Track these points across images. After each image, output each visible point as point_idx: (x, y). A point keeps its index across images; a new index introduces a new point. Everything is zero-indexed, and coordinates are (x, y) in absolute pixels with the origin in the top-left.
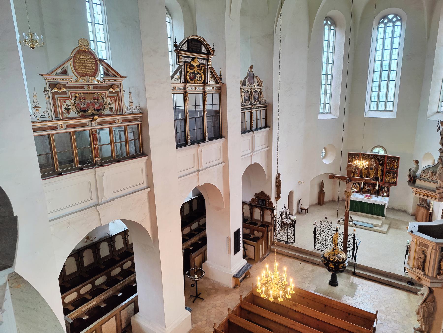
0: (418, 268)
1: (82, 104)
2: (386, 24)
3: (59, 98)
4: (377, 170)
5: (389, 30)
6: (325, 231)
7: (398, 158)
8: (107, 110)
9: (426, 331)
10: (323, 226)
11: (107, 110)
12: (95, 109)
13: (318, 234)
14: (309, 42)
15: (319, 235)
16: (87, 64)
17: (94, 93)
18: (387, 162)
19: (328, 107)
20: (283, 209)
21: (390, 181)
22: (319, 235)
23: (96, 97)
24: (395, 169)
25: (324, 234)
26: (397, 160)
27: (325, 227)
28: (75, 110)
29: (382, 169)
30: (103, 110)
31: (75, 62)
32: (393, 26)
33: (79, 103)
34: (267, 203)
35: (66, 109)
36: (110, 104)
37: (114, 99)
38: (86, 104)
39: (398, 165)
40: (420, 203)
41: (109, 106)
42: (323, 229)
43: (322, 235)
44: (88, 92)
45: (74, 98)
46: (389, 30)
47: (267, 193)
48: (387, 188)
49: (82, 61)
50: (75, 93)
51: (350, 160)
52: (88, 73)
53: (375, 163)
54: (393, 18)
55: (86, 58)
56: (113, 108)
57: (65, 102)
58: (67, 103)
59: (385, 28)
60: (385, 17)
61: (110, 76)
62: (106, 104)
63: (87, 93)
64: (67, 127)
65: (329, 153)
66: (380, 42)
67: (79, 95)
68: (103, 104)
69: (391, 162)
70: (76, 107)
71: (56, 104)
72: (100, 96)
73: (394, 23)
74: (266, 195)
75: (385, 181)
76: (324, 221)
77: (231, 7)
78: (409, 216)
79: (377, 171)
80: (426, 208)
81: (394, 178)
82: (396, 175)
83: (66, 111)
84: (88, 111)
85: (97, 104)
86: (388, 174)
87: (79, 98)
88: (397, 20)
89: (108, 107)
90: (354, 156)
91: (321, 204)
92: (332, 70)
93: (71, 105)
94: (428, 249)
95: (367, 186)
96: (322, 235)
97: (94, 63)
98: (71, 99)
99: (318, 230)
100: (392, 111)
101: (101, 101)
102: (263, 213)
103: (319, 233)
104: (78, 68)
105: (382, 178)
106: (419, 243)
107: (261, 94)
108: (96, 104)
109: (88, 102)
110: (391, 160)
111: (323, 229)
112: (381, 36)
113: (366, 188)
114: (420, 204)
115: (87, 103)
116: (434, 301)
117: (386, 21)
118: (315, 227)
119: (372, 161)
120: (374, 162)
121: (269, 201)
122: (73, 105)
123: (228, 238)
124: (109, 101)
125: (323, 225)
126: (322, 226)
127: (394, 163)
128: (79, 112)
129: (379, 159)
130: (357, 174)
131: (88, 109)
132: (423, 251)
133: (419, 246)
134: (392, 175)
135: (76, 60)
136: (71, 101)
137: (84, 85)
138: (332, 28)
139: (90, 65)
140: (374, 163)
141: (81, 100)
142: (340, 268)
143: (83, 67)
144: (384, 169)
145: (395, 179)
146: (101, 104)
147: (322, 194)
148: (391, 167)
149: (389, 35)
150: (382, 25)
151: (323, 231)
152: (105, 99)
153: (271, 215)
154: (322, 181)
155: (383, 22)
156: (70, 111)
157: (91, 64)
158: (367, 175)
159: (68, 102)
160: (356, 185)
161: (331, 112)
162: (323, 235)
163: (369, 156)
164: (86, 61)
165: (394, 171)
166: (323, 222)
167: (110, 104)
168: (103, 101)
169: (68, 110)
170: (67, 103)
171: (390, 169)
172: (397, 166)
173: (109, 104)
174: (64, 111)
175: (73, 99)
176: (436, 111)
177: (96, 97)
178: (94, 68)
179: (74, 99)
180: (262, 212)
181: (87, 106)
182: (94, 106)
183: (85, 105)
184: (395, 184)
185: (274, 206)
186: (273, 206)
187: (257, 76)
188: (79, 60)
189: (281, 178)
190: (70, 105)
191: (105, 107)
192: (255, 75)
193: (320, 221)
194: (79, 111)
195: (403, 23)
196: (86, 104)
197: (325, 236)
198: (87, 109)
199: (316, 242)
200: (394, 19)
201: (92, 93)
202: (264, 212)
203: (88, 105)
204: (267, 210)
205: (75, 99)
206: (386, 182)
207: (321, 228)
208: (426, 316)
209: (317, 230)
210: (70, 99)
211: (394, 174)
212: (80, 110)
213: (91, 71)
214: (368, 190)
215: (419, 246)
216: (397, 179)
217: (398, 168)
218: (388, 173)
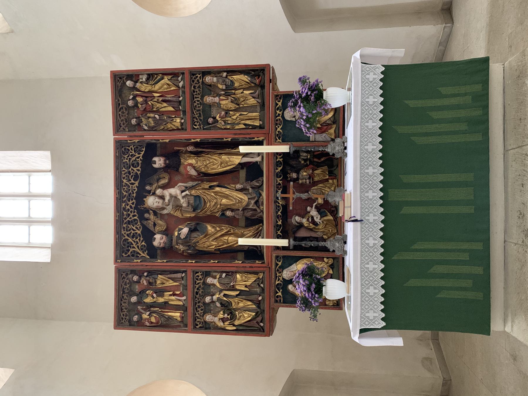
18: (152, 129)
21: (252, 101)
24: (181, 84)
26: (129, 83)
29: (190, 148)
51: (153, 320)
53: (165, 187)
75: (254, 127)
79: (206, 174)
82: (208, 79)
86: (214, 118)
90: (134, 299)
95: (298, 218)
113: (312, 226)
119: (156, 205)
120: (159, 192)
127: (148, 96)
129: (137, 170)
130: (231, 274)
134: (217, 99)
140: (167, 193)
148: (171, 109)
160: (290, 282)
163: (129, 223)
165: (187, 90)
172: (162, 78)
206: (257, 123)
211: (210, 89)
214: (322, 215)
216: (232, 71)
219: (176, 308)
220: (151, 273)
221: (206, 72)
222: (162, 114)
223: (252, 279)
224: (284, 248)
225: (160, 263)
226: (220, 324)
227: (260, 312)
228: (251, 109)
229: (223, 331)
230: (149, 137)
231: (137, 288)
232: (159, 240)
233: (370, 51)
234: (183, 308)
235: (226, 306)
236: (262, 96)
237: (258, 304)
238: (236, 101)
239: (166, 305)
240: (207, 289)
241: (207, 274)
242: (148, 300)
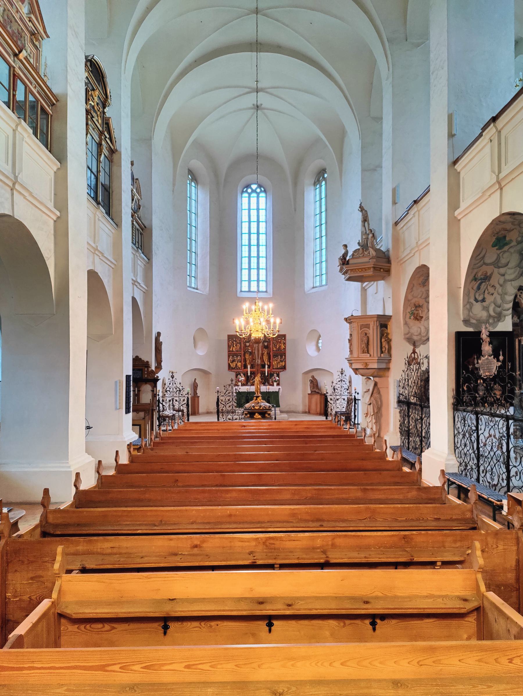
0: (363, 352)
2: (250, 194)
4: (263, 354)
5: (254, 200)
6: (231, 400)
7: (284, 336)
9: (377, 431)
10: (229, 393)
13: (223, 406)
14: (174, 185)
15: (223, 407)
18: (273, 343)
19: (194, 282)
20: (170, 380)
21: (279, 366)
22: (223, 407)
25: (230, 404)
26: (283, 338)
27: (231, 394)
32: (258, 197)
34: (146, 372)
39: (285, 344)
40: (311, 390)
42: (229, 398)
43: (228, 406)
46: (254, 200)
47: (145, 358)
48: (276, 374)
54: (257, 188)
59: (249, 197)
60: (248, 186)
65: (200, 344)
66: (245, 213)
69: (277, 342)
73: (258, 194)
74: (143, 361)
76: (229, 385)
77: (126, 62)
78: (299, 414)
80: (318, 393)
81: (282, 362)
82: (284, 357)
88: (261, 191)
91: (195, 413)
92: (196, 234)
94: (369, 328)
96: (228, 406)
99: (222, 400)
100: (266, 292)
102: (139, 391)
103: (224, 405)
105: (269, 364)
106: (361, 326)
107: (139, 208)
110: (277, 339)
111: (229, 398)
112: (245, 206)
114: (312, 392)
116: (379, 393)
117: (249, 190)
118: (218, 397)
121: (148, 370)
123: (121, 382)
125: (228, 392)
126: (227, 393)
127: (280, 342)
130: (241, 362)
132: (366, 334)
133: (361, 330)
138: (193, 184)
142: (268, 416)
144: (270, 352)
145: (284, 363)
147: (196, 398)
149: (254, 206)
150: (245, 195)
151: (229, 400)
153: (153, 391)
154: (195, 379)
155: (246, 191)
158: (252, 363)
161: (198, 288)
162: (230, 406)
166: (228, 387)
171: (276, 351)
176: (312, 286)
180: (136, 389)
184: (284, 368)
185: (158, 377)
186: (156, 377)
187: (137, 179)
189: (161, 339)
192: (135, 178)
193: (225, 387)
195: (268, 194)
197: (231, 407)
199: (220, 418)
200: (258, 190)
202: (141, 389)
204: (146, 384)
207: (225, 397)
208: (376, 411)
209: (220, 400)
211: (281, 357)
215: (361, 330)
216: (285, 362)
217: (285, 349)
218: (275, 356)
219: (233, 349)
220: (240, 343)
221: (285, 356)
222: (276, 346)
223: (240, 367)
224: (248, 374)
225: (242, 345)
226: (230, 359)
227: (233, 369)
228: (277, 366)
229: (229, 360)
230: (271, 342)
231: (237, 339)
232: (248, 344)
233: (281, 389)
234: (233, 351)
235: (233, 361)
236: (280, 369)
237: (234, 368)
238: (279, 363)
239: (233, 346)
240: (237, 356)
241: (241, 356)
242: (234, 342)
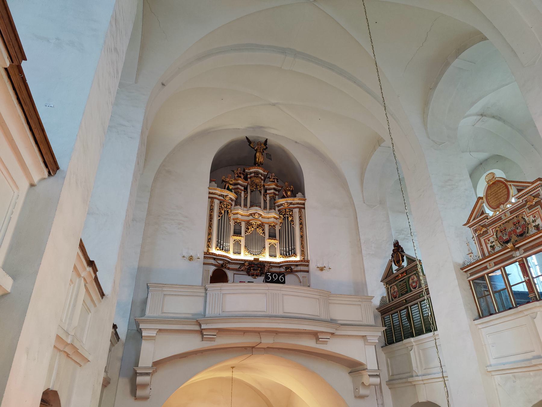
1: (504, 236)
3: (483, 239)
8: (532, 230)
11: (532, 230)
12: (517, 235)
16: (499, 193)
17: (513, 218)
23: (516, 222)
28: (499, 245)
30: (528, 233)
31: (488, 199)
33: (501, 236)
35: (491, 246)
36: (534, 221)
37: (537, 213)
38: (507, 234)
41: (534, 224)
44: (507, 221)
45: (495, 233)
49: (493, 194)
50: (496, 228)
52: (502, 201)
55: (496, 189)
56: (539, 225)
57: (489, 241)
58: (491, 241)
61: (524, 189)
62: (529, 224)
63: (506, 222)
64: (495, 264)
67: (499, 228)
68: (526, 225)
70: (499, 241)
71: (482, 245)
72: (521, 218)
83: (492, 248)
84: (511, 240)
85: (519, 228)
87: (500, 230)
89: (532, 226)
93: (494, 240)
97: (505, 188)
98: (493, 235)
101: (522, 222)
104: (492, 203)
108: (518, 229)
109: (508, 231)
115: (508, 233)
122: (496, 240)
124: (532, 218)
128: (502, 245)
131: (510, 238)
135: (489, 197)
136: (493, 237)
137: (500, 216)
139: (501, 193)
141: (502, 232)
143: (496, 199)
146: (523, 227)
152: (527, 219)
156: (494, 247)
157: (502, 191)
159: (492, 239)
164: (497, 191)
167: (534, 221)
168: (524, 222)
169: (493, 247)
170: (491, 241)
173: (532, 222)
174: (490, 249)
175: (495, 234)
177: (516, 222)
178: (507, 192)
179: (496, 234)
181: (509, 236)
182: (516, 232)
183: (506, 235)
188: (491, 195)
190: (494, 242)
191: (528, 227)
194: (502, 244)
196: (507, 234)
198: (510, 239)
201: (511, 219)
203: (510, 233)
205: (496, 234)
210: (492, 235)
212: (503, 243)
213: (503, 199)
